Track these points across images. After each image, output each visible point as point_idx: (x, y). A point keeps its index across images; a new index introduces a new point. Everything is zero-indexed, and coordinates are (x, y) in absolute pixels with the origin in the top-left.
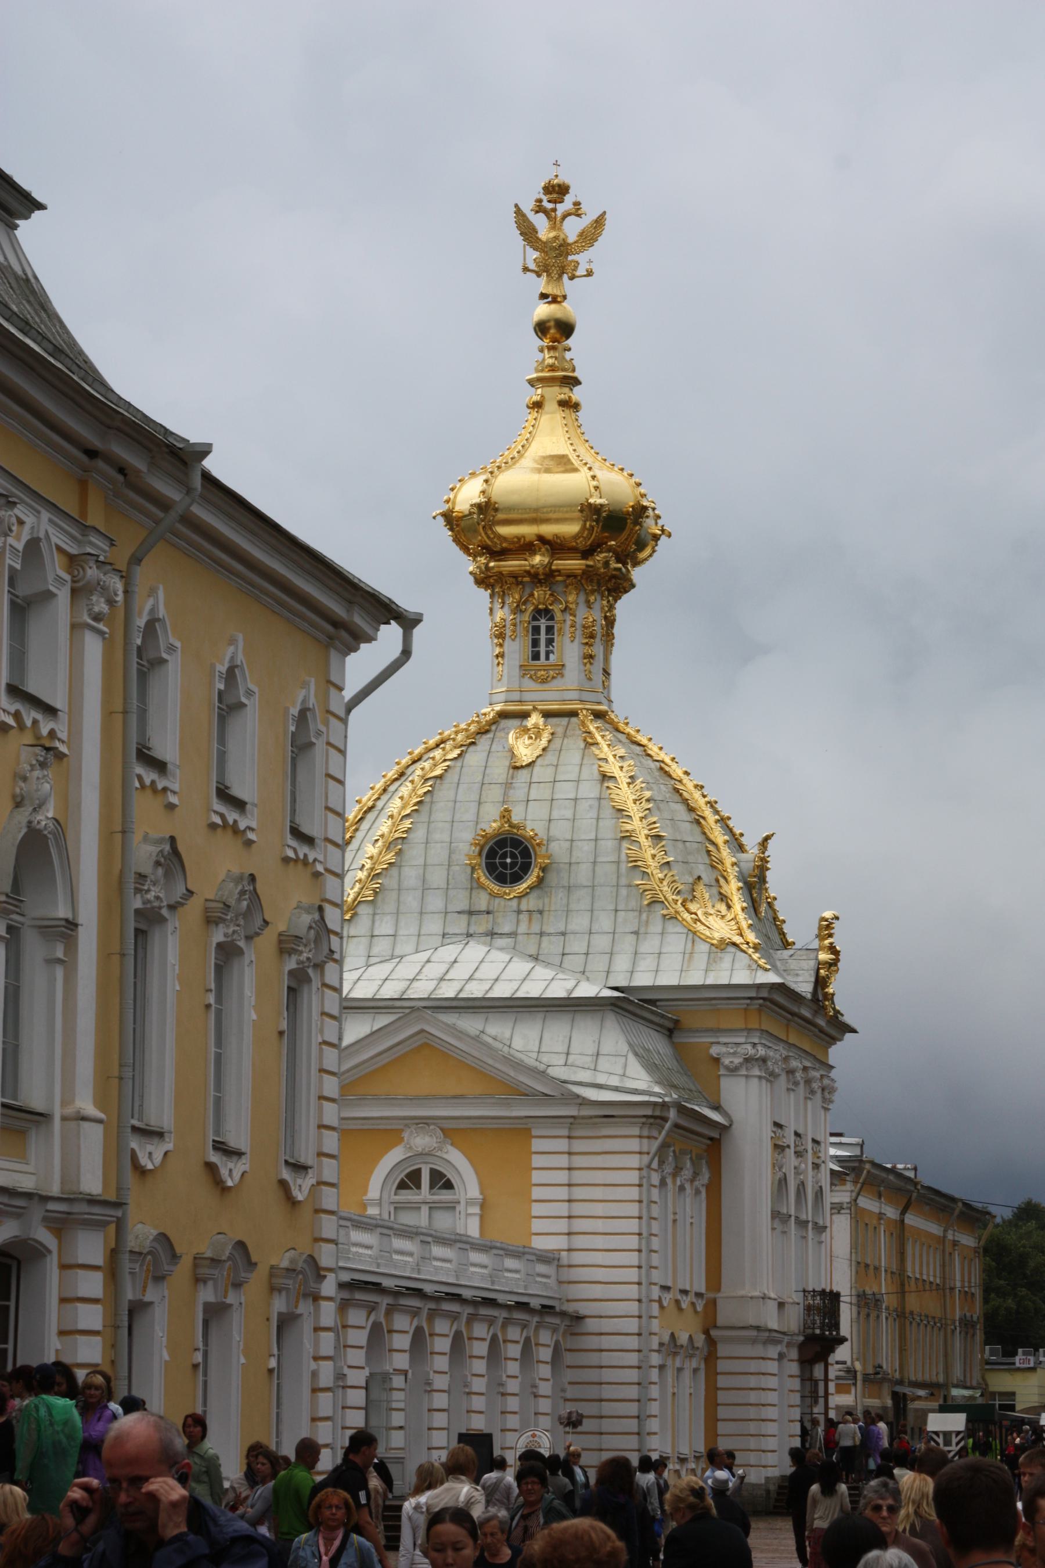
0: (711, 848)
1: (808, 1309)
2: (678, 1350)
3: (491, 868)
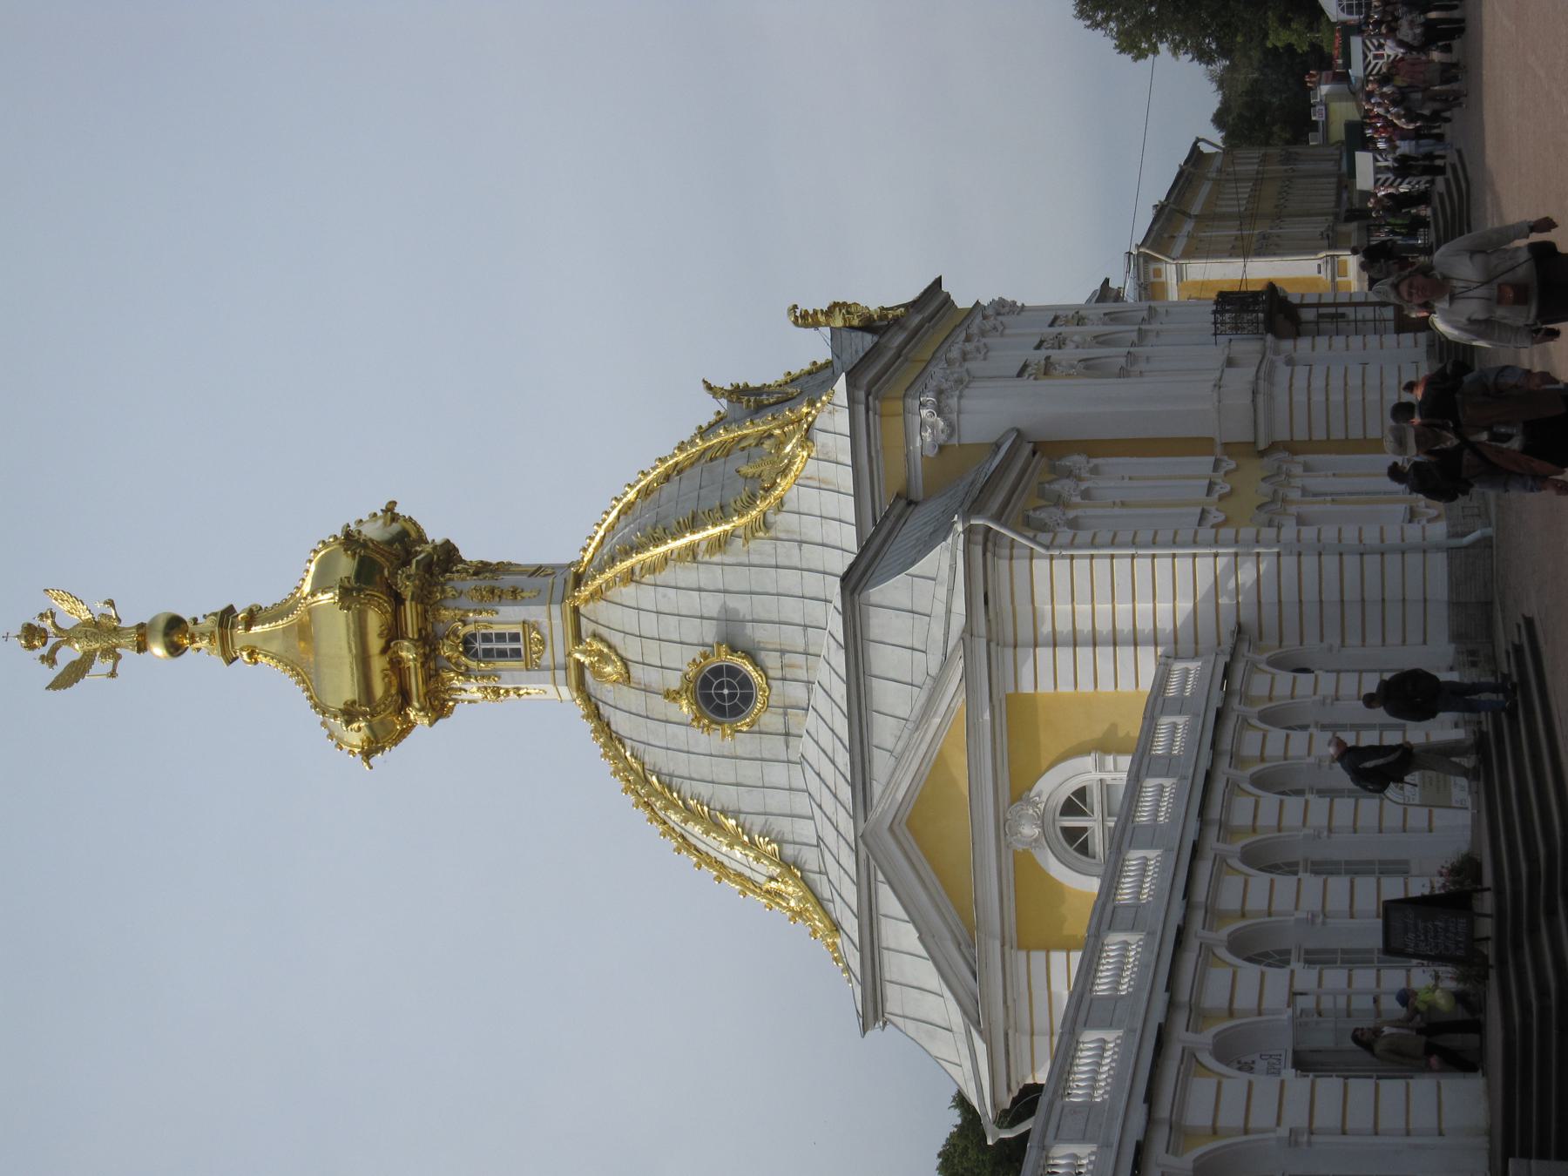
0: (708, 456)
1: (1237, 328)
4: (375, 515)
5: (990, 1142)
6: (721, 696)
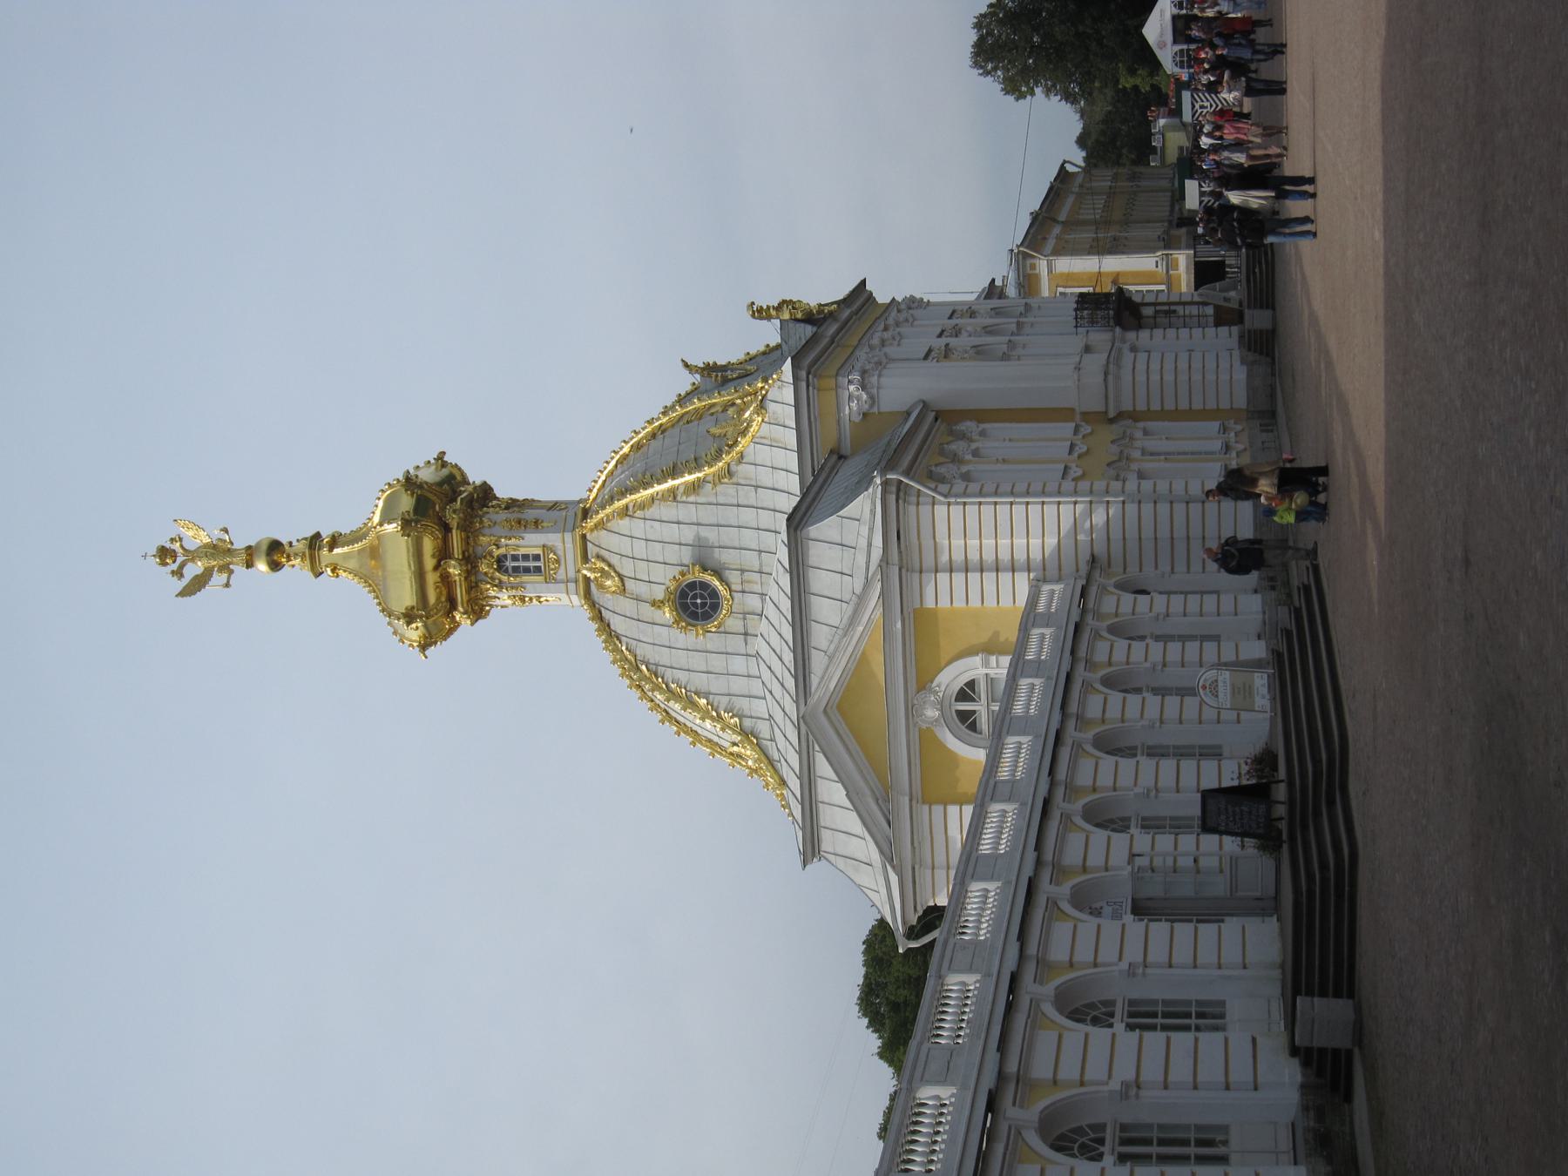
1: (1093, 322)
2: (1125, 455)
4: (429, 462)
5: (901, 951)
6: (695, 605)
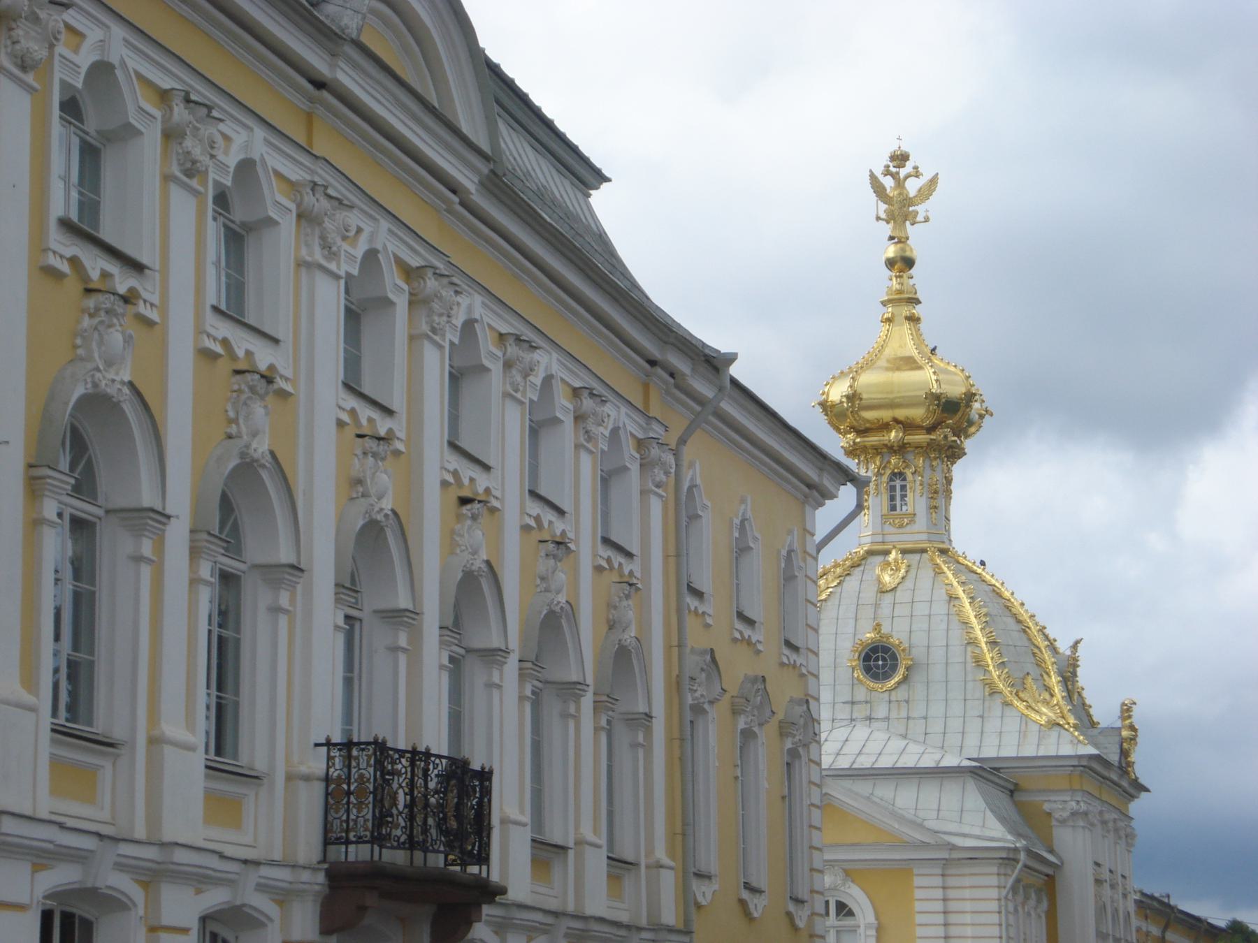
0: (1036, 650)
3: (868, 670)
6: (877, 659)
